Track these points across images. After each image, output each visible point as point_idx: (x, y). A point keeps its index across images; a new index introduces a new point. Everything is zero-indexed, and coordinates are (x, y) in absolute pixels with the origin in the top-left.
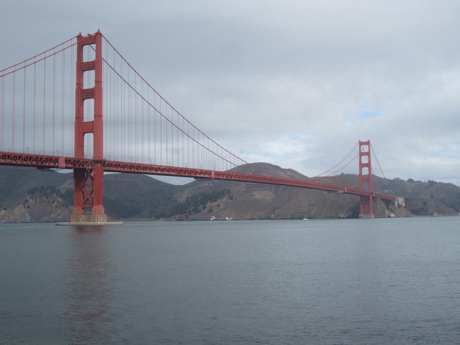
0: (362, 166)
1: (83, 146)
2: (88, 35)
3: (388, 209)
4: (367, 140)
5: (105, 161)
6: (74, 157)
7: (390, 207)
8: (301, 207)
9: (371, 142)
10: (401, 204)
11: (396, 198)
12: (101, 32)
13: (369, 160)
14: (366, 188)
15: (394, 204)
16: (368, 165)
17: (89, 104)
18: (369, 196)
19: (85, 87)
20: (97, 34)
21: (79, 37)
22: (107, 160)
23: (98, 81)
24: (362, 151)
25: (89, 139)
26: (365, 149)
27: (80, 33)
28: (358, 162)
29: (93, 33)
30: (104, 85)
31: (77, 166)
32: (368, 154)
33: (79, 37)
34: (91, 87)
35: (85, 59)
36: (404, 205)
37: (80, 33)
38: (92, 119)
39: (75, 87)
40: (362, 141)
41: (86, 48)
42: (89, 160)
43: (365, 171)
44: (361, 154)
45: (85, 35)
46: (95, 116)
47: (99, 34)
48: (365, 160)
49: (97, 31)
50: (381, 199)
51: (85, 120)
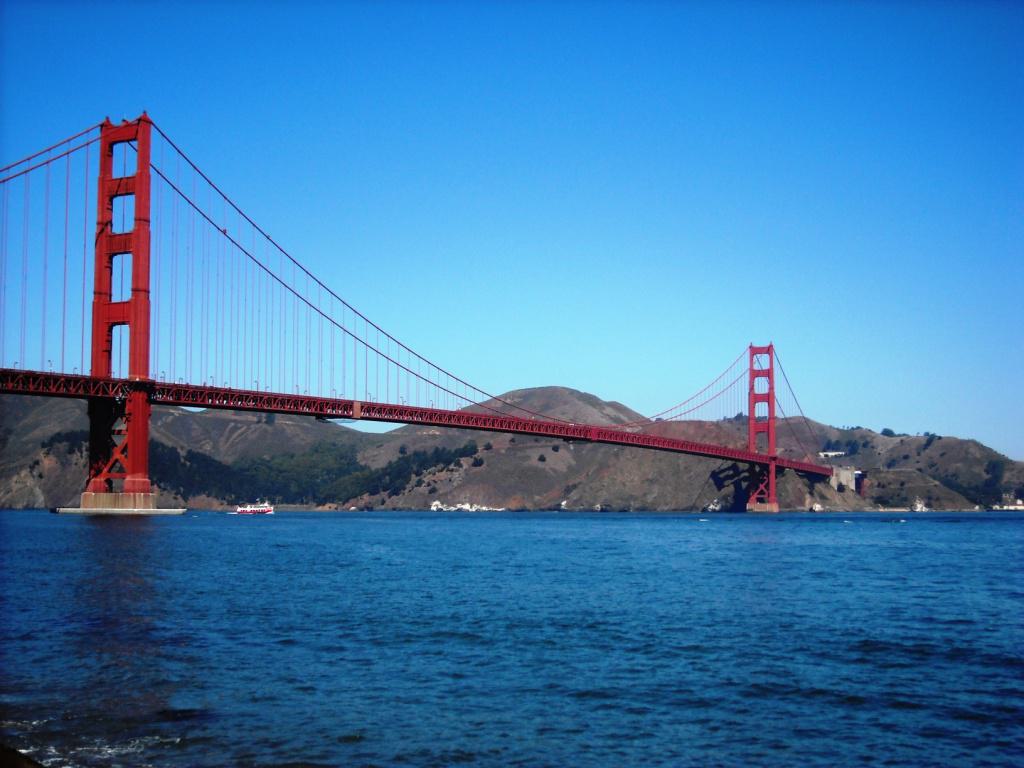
0: (755, 398)
1: (109, 352)
2: (124, 121)
3: (811, 494)
4: (767, 344)
5: (153, 383)
6: (87, 372)
7: (819, 487)
8: (624, 485)
9: (776, 348)
10: (844, 483)
11: (835, 471)
12: (151, 116)
13: (771, 388)
14: (760, 449)
15: (828, 483)
16: (769, 398)
17: (123, 265)
18: (768, 466)
19: (117, 229)
20: (139, 120)
21: (105, 126)
22: (159, 380)
23: (143, 220)
24: (756, 367)
25: (121, 335)
26: (763, 362)
27: (107, 118)
28: (747, 391)
29: (131, 119)
30: (153, 227)
31: (92, 393)
32: (768, 374)
33: (105, 126)
34: (127, 231)
35: (117, 173)
36: (852, 486)
37: (107, 118)
38: (127, 296)
39: (93, 229)
40: (757, 344)
41: (118, 148)
42: (120, 381)
43: (761, 410)
44: (755, 374)
45: (116, 122)
46: (135, 290)
47: (144, 122)
48: (761, 385)
49: (139, 115)
50: (796, 470)
51: (116, 298)
